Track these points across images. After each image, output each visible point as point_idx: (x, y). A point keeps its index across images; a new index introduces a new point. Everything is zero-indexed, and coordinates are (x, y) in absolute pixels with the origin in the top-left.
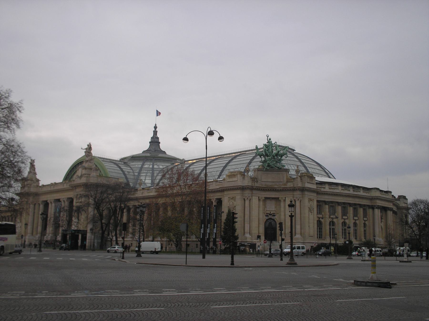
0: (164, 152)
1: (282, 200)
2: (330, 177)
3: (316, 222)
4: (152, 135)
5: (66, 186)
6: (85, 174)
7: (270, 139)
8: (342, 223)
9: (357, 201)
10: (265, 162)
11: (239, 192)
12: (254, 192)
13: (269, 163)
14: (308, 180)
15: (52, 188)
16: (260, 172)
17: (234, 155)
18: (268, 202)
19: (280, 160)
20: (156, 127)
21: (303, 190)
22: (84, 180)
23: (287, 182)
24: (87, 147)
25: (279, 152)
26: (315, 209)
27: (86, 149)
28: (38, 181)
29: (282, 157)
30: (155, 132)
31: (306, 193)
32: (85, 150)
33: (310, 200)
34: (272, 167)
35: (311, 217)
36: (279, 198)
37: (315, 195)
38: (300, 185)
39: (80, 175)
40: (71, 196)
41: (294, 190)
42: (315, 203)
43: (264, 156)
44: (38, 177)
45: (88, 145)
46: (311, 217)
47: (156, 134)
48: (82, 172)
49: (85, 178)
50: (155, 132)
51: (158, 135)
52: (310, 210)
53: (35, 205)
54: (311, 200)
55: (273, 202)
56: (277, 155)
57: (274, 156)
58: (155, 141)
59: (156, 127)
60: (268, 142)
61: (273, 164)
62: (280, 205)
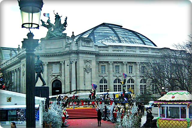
1: (62, 64)
2: (145, 44)
14: (83, 44)
18: (54, 66)
21: (77, 53)
23: (66, 47)
31: (80, 55)
36: (60, 62)
37: (94, 56)
38: (74, 48)
41: (70, 53)
46: (88, 76)
52: (87, 70)
54: (88, 62)
55: (58, 65)
61: (55, 33)
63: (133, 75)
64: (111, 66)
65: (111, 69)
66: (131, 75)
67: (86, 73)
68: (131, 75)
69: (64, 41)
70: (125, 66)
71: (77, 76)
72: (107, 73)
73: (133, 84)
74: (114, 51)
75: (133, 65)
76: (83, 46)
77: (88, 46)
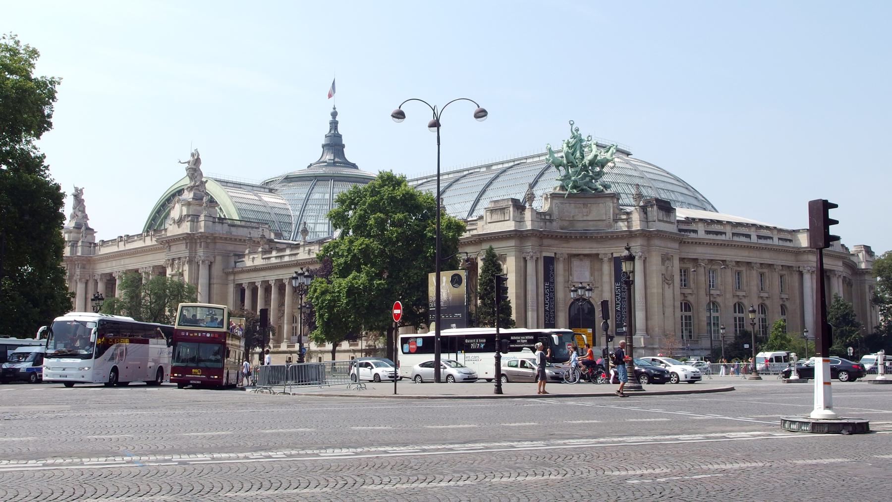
0: (354, 166)
3: (678, 304)
4: (326, 129)
5: (149, 242)
6: (189, 216)
7: (577, 130)
8: (735, 305)
9: (766, 258)
10: (567, 177)
11: (512, 243)
12: (546, 242)
13: (575, 181)
14: (661, 214)
15: (122, 247)
16: (555, 201)
17: (500, 166)
18: (576, 263)
19: (600, 174)
20: (334, 114)
22: (186, 228)
24: (189, 158)
25: (596, 156)
26: (677, 278)
27: (189, 162)
28: (90, 231)
29: (603, 167)
30: (334, 125)
31: (656, 242)
32: (187, 165)
33: (666, 258)
34: (582, 190)
35: (669, 292)
36: (598, 255)
37: (676, 245)
39: (177, 218)
40: (162, 262)
42: (676, 263)
43: (564, 166)
44: (91, 224)
45: (193, 155)
46: (669, 292)
47: (336, 128)
48: (181, 211)
49: (189, 224)
50: (334, 125)
51: (340, 130)
52: (667, 280)
53: (86, 283)
54: (668, 259)
55: (587, 263)
56: (593, 163)
57: (585, 166)
58: (335, 144)
59: (334, 114)
60: (574, 137)
61: (585, 184)
62: (601, 270)
63: (744, 294)
64: (701, 270)
65: (702, 279)
66: (741, 294)
67: (667, 286)
68: (741, 294)
69: (611, 205)
70: (729, 272)
71: (648, 291)
72: (692, 285)
73: (741, 315)
74: (708, 232)
75: (743, 269)
76: (659, 221)
77: (666, 222)
